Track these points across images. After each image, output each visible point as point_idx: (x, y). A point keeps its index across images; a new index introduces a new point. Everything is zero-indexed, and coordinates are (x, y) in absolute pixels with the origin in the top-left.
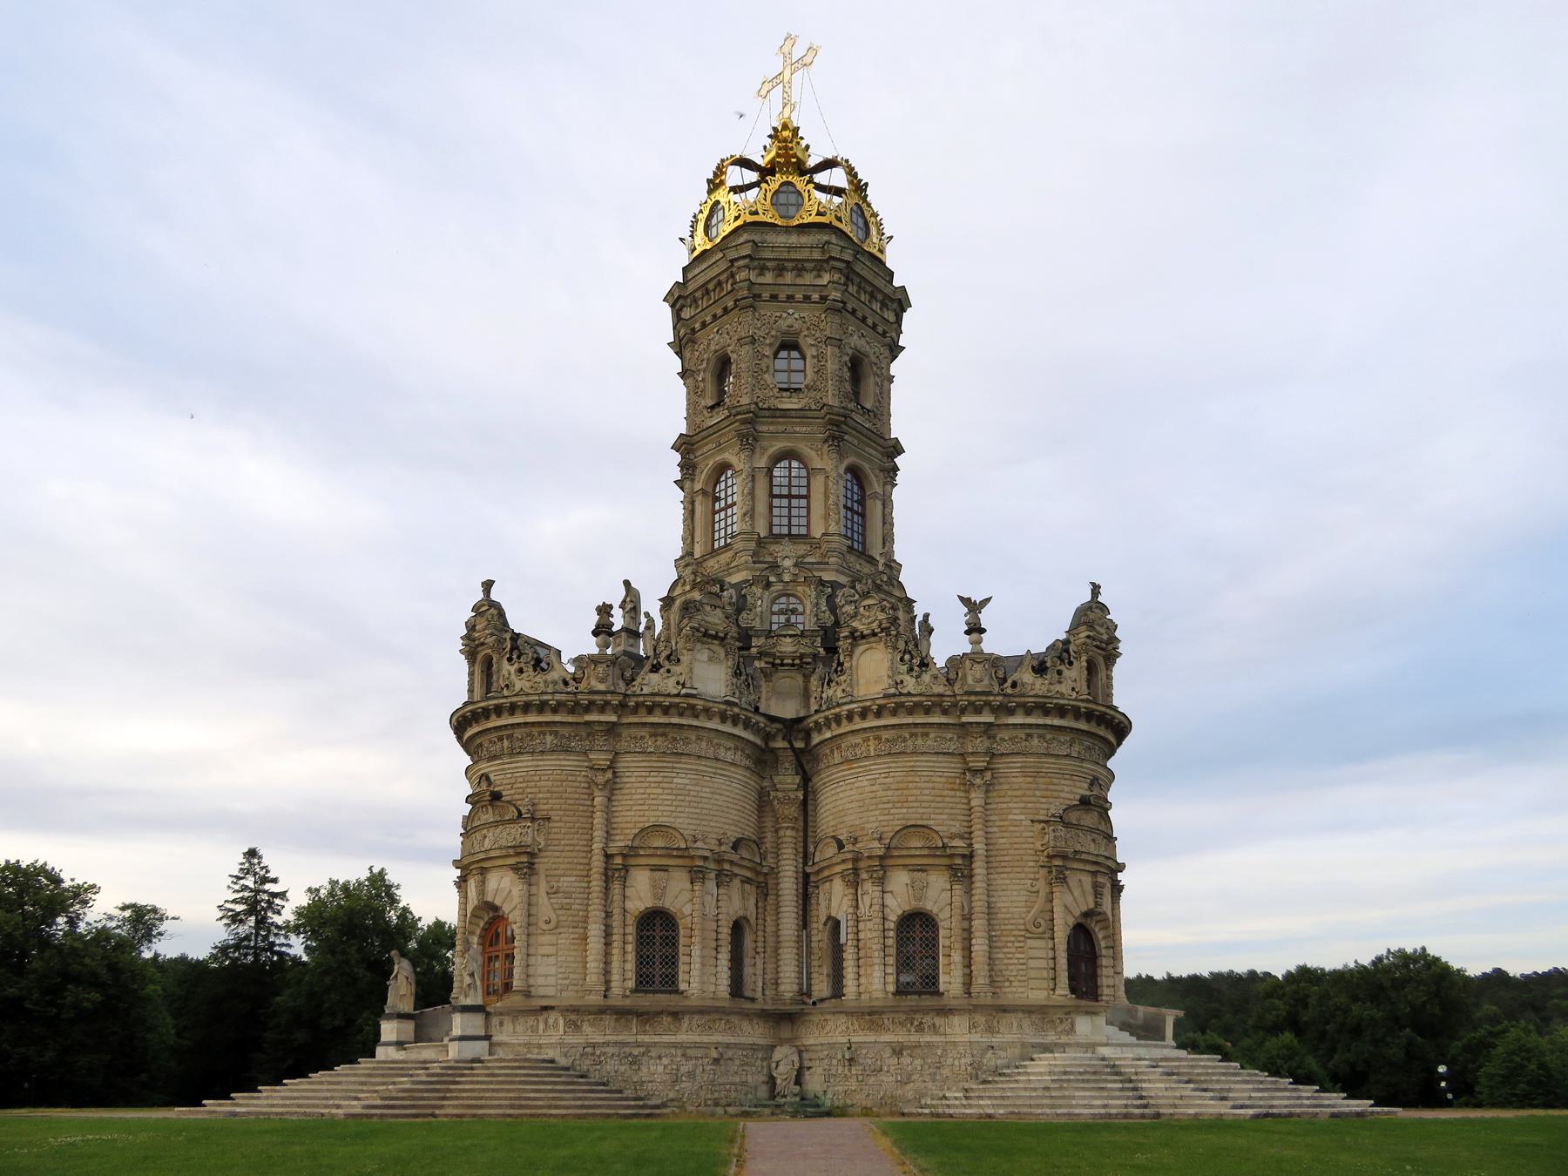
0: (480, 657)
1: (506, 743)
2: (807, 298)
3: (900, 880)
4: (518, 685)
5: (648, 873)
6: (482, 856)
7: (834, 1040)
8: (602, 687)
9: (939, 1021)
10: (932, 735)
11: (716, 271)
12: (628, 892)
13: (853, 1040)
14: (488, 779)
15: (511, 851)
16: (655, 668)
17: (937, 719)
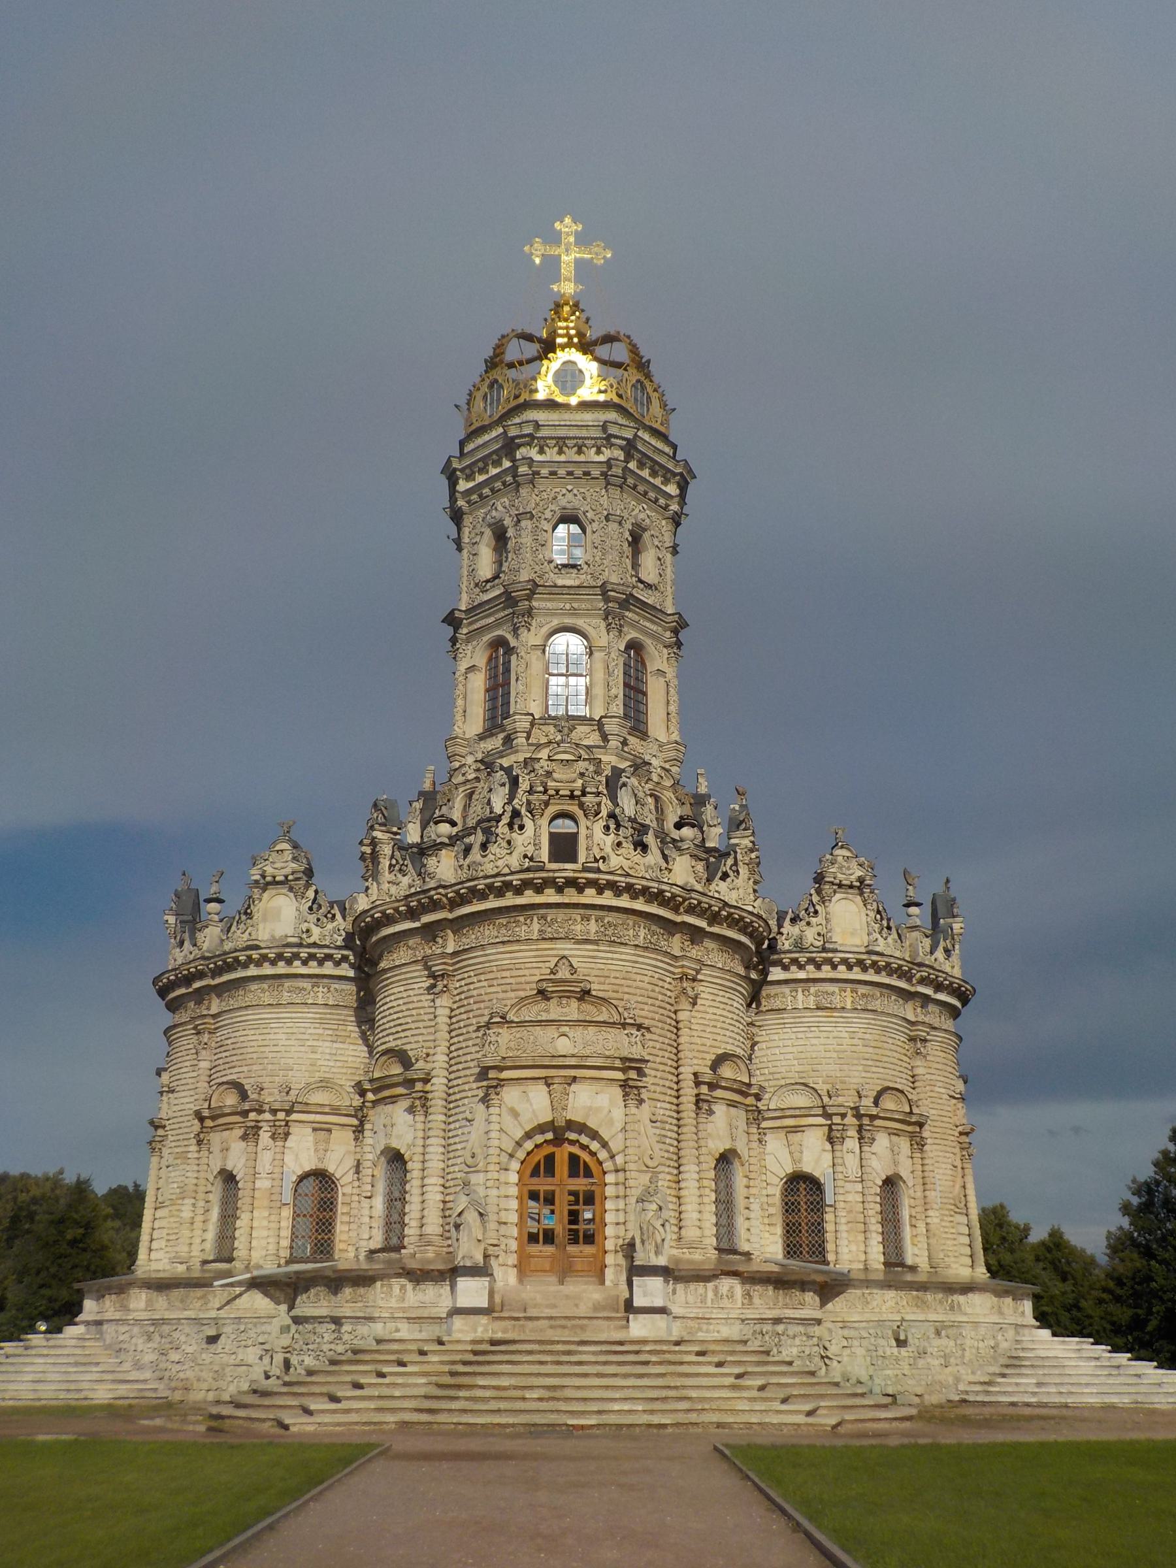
0: (552, 810)
1: (593, 927)
2: (656, 501)
3: (882, 1141)
4: (615, 861)
5: (724, 1108)
6: (573, 1061)
7: (884, 1317)
8: (698, 887)
9: (962, 1299)
10: (893, 998)
11: (584, 433)
12: (710, 1127)
13: (907, 1317)
14: (571, 965)
15: (618, 1064)
16: (725, 876)
17: (902, 984)
